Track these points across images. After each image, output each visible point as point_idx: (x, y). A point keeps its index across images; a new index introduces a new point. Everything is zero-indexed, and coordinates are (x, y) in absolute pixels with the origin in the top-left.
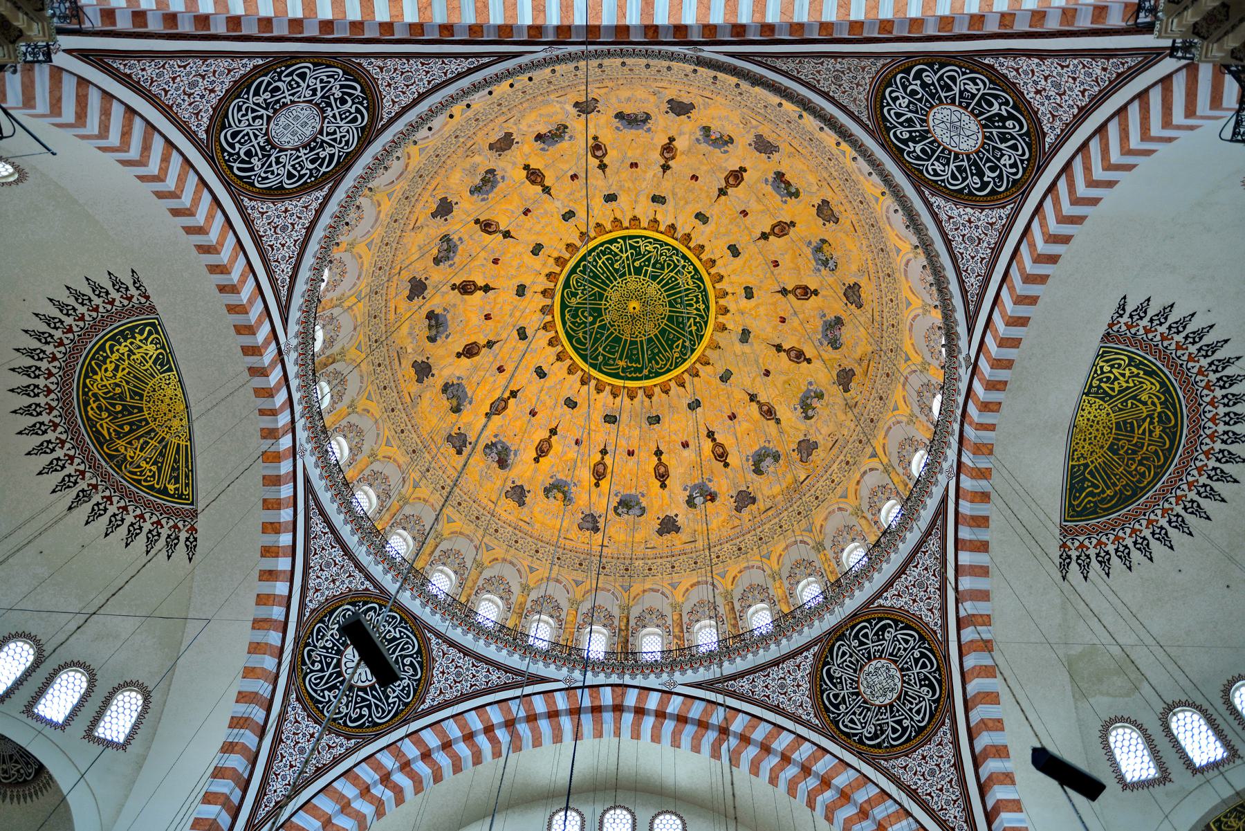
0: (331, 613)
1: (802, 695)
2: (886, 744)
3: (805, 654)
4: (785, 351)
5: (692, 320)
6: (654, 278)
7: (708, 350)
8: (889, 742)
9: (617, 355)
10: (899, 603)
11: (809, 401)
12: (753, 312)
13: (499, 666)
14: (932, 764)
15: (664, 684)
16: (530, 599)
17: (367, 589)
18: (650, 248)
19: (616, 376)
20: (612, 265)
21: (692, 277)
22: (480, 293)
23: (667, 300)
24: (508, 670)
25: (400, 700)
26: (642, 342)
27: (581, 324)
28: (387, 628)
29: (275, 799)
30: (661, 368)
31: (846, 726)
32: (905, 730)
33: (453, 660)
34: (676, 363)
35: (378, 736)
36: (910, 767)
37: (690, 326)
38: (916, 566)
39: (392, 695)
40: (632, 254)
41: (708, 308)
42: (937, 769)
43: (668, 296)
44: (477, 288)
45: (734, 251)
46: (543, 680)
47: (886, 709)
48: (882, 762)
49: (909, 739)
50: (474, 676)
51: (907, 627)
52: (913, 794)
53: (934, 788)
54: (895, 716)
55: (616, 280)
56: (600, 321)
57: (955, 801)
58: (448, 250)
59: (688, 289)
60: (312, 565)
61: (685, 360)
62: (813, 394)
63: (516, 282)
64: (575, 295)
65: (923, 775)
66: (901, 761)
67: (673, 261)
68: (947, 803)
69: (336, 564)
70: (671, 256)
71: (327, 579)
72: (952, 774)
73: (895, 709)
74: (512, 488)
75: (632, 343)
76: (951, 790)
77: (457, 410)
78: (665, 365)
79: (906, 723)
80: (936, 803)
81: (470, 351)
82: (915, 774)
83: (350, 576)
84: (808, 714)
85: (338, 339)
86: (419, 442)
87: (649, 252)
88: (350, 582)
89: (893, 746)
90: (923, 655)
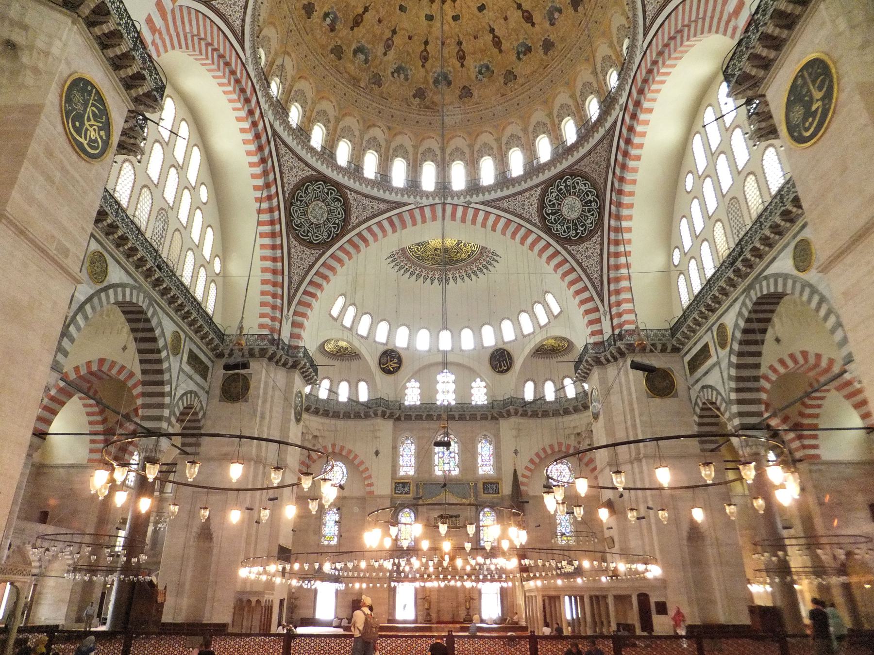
1: (294, 181)
4: (425, 47)
10: (351, 201)
13: (243, 21)
14: (304, 256)
24: (243, 26)
32: (307, 236)
36: (298, 249)
49: (305, 240)
52: (290, 258)
66: (296, 243)
72: (306, 267)
79: (310, 234)
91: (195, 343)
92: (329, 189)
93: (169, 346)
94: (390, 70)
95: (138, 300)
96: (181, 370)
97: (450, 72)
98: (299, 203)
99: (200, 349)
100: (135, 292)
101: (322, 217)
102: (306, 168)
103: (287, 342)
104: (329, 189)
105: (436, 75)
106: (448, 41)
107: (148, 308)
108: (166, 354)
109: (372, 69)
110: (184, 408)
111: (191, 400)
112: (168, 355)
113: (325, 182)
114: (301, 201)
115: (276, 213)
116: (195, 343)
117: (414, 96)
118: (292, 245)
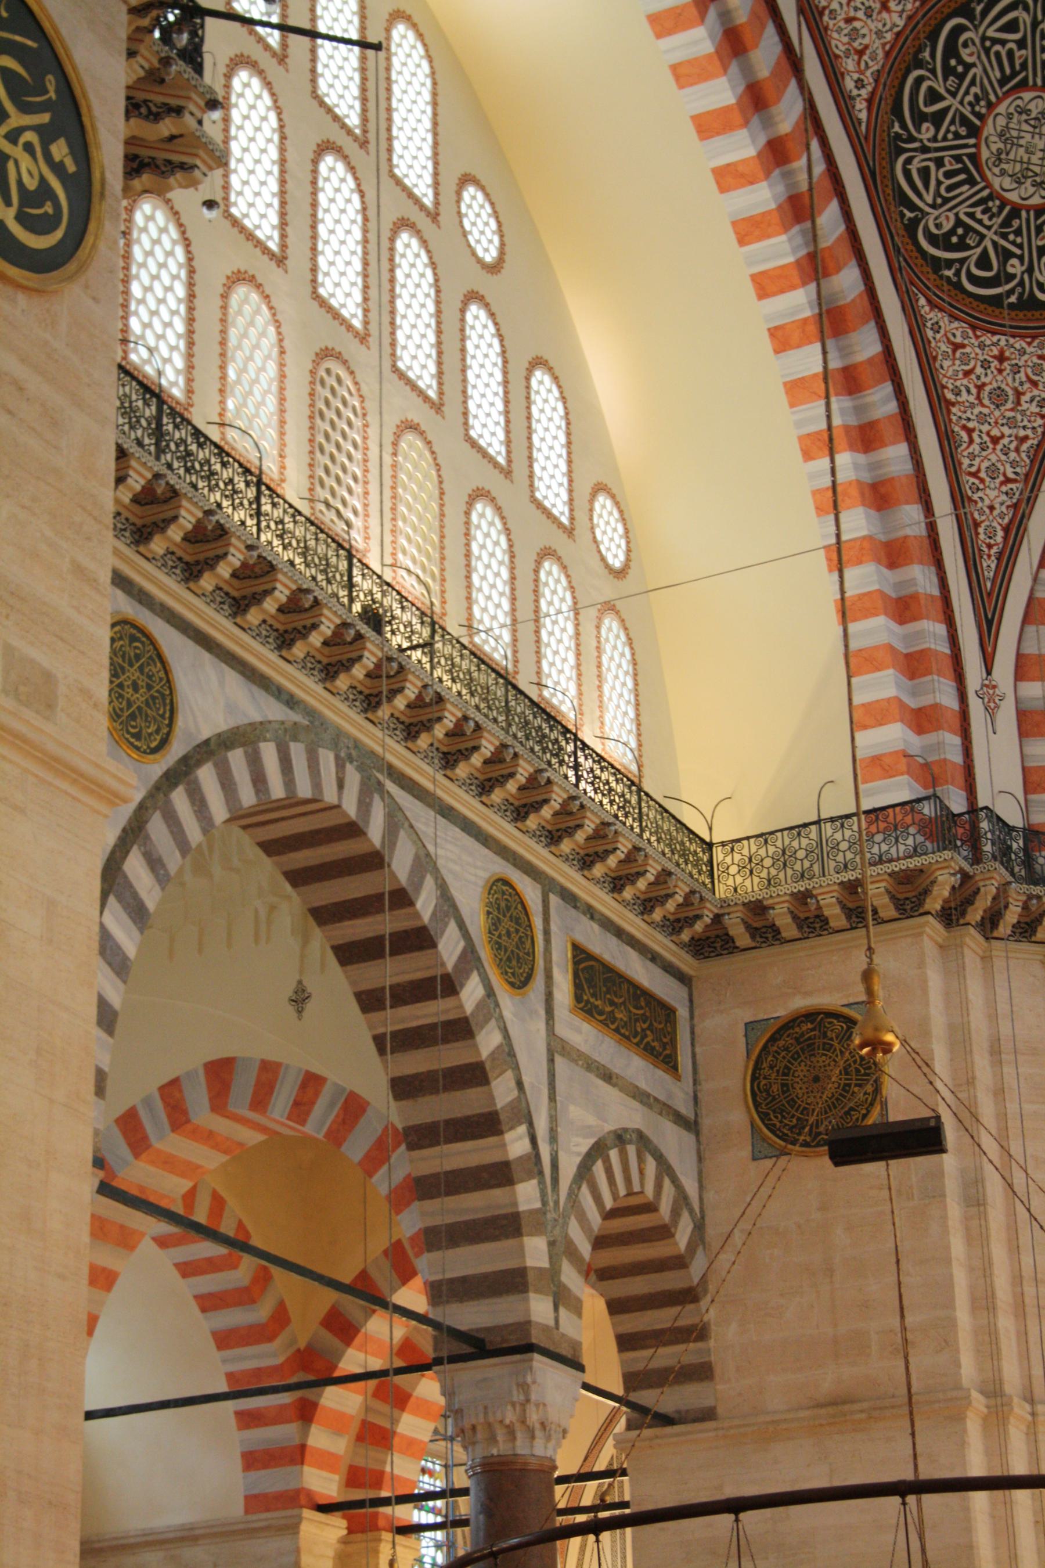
2: (949, 273)
8: (958, 273)
14: (1007, 383)
31: (907, 174)
42: (1011, 397)
47: (1001, 209)
48: (922, 301)
49: (996, 301)
52: (939, 405)
53: (985, 428)
54: (1004, 236)
57: (1008, 481)
65: (980, 388)
66: (957, 329)
68: (993, 471)
73: (1016, 223)
76: (1013, 455)
80: (972, 456)
82: (967, 374)
84: (860, 84)
89: (958, 286)
91: (590, 912)
93: (485, 953)
95: (317, 785)
96: (557, 1047)
98: (927, 131)
99: (619, 933)
100: (297, 751)
103: (1015, 819)
107: (364, 806)
108: (480, 992)
110: (609, 1215)
111: (628, 1180)
112: (490, 993)
114: (937, 119)
115: (829, 218)
116: (590, 912)
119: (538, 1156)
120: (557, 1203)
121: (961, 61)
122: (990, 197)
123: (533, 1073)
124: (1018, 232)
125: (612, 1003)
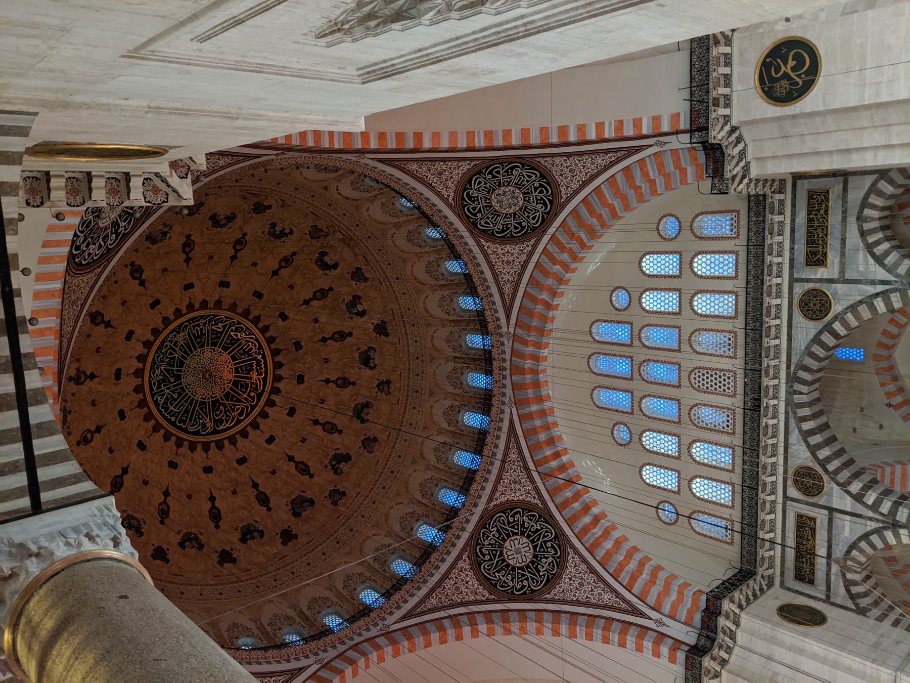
0: (489, 580)
3: (486, 248)
5: (213, 327)
6: (181, 364)
7: (237, 311)
9: (248, 381)
11: (278, 233)
12: (204, 281)
15: (508, 340)
16: (448, 428)
17: (468, 557)
18: (158, 372)
19: (265, 379)
20: (175, 400)
21: (179, 333)
22: (218, 504)
23: (199, 350)
24: (507, 448)
25: (538, 521)
26: (235, 364)
27: (227, 416)
28: (492, 537)
29: (614, 599)
30: (255, 346)
31: (537, 222)
33: (506, 487)
34: (250, 334)
35: (564, 534)
37: (219, 328)
38: (427, 177)
39: (535, 527)
40: (164, 386)
41: (202, 317)
43: (195, 349)
44: (214, 507)
45: (155, 304)
46: (512, 422)
50: (515, 471)
51: (470, 182)
54: (532, 191)
55: (187, 394)
56: (222, 400)
57: (592, 159)
58: (190, 540)
59: (189, 334)
60: (459, 600)
61: (247, 328)
62: (271, 230)
63: (203, 476)
64: (204, 425)
65: (573, 176)
66: (563, 190)
67: (167, 351)
68: (593, 163)
69: (456, 583)
70: (163, 354)
71: (467, 588)
74: (365, 449)
75: (237, 371)
77: (312, 502)
78: (252, 343)
80: (592, 170)
81: (263, 500)
83: (461, 571)
84: (528, 246)
85: (284, 614)
86: (343, 528)
87: (161, 371)
88: (466, 570)
89: (552, 194)
90: (491, 172)
92: (475, 215)
94: (293, 237)
97: (208, 228)
99: (793, 230)
101: (504, 192)
102: (489, 251)
104: (475, 215)
105: (230, 225)
106: (204, 260)
109: (319, 244)
112: (836, 318)
113: (475, 224)
117: (270, 207)
118: (570, 191)
119: (882, 292)
120: (895, 281)
121: (503, 227)
122: (525, 201)
123: (856, 293)
124: (528, 189)
125: (818, 241)
